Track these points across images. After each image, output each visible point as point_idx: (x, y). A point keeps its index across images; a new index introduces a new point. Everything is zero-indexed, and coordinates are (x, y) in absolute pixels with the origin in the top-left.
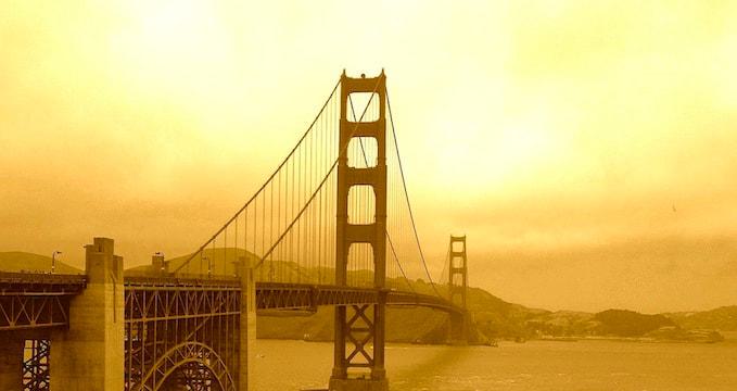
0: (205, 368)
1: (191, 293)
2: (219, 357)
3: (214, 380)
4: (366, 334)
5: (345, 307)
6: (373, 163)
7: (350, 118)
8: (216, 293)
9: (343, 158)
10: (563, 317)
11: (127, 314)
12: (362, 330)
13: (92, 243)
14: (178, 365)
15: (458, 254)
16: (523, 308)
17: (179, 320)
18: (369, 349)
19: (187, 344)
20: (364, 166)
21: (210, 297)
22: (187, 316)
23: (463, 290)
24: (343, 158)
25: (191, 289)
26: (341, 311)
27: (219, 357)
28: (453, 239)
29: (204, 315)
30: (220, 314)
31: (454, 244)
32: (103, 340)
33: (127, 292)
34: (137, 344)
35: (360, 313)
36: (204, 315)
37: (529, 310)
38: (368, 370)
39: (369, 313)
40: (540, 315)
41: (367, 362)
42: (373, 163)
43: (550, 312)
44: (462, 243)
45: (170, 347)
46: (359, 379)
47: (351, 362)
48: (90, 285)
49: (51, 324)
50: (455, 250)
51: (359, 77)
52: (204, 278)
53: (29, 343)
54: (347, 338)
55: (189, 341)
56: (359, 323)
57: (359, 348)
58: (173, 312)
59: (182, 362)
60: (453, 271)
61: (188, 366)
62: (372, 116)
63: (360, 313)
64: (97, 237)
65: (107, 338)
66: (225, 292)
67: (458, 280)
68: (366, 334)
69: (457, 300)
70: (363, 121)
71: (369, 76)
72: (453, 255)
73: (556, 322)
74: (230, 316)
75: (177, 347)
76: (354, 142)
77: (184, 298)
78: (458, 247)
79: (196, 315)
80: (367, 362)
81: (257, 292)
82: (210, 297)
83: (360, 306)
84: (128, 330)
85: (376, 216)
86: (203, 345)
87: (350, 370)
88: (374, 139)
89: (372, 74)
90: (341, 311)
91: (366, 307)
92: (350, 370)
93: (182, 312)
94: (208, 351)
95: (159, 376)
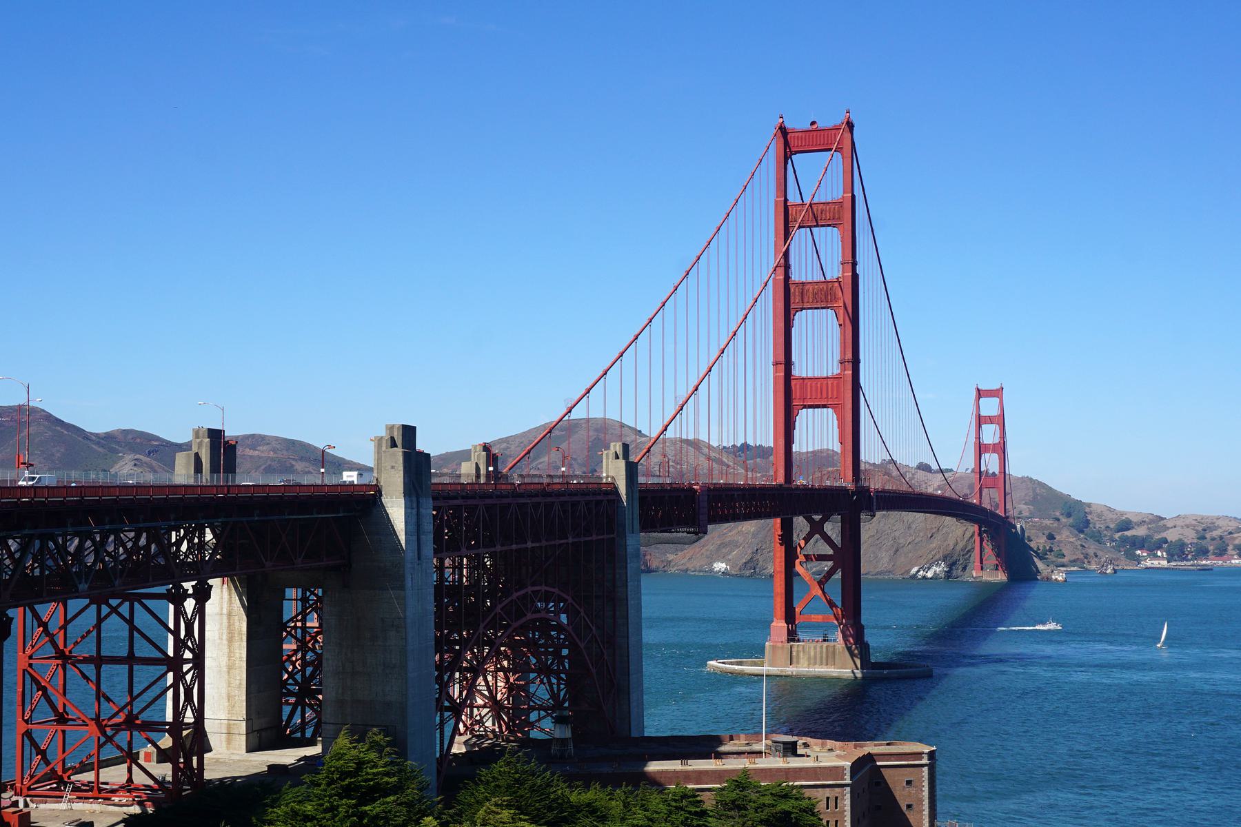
0: (560, 628)
2: (582, 610)
3: (573, 647)
5: (792, 519)
6: (834, 271)
7: (793, 198)
8: (574, 505)
10: (1188, 526)
12: (821, 558)
15: (990, 420)
16: (1111, 510)
19: (530, 589)
20: (818, 277)
22: (529, 545)
23: (1002, 480)
25: (535, 500)
26: (787, 528)
27: (582, 610)
28: (980, 394)
29: (558, 542)
30: (582, 539)
32: (402, 588)
34: (455, 590)
36: (558, 542)
37: (1122, 515)
39: (833, 528)
42: (834, 271)
43: (1162, 519)
44: (996, 400)
50: (982, 414)
51: (807, 126)
53: (291, 593)
59: (523, 620)
60: (981, 449)
62: (833, 191)
63: (817, 529)
65: (409, 583)
66: (587, 503)
67: (991, 463)
68: (827, 565)
69: (989, 499)
70: (816, 200)
71: (821, 124)
72: (980, 421)
73: (1172, 536)
75: (515, 595)
78: (989, 407)
79: (544, 543)
85: (842, 362)
89: (830, 119)
90: (787, 528)
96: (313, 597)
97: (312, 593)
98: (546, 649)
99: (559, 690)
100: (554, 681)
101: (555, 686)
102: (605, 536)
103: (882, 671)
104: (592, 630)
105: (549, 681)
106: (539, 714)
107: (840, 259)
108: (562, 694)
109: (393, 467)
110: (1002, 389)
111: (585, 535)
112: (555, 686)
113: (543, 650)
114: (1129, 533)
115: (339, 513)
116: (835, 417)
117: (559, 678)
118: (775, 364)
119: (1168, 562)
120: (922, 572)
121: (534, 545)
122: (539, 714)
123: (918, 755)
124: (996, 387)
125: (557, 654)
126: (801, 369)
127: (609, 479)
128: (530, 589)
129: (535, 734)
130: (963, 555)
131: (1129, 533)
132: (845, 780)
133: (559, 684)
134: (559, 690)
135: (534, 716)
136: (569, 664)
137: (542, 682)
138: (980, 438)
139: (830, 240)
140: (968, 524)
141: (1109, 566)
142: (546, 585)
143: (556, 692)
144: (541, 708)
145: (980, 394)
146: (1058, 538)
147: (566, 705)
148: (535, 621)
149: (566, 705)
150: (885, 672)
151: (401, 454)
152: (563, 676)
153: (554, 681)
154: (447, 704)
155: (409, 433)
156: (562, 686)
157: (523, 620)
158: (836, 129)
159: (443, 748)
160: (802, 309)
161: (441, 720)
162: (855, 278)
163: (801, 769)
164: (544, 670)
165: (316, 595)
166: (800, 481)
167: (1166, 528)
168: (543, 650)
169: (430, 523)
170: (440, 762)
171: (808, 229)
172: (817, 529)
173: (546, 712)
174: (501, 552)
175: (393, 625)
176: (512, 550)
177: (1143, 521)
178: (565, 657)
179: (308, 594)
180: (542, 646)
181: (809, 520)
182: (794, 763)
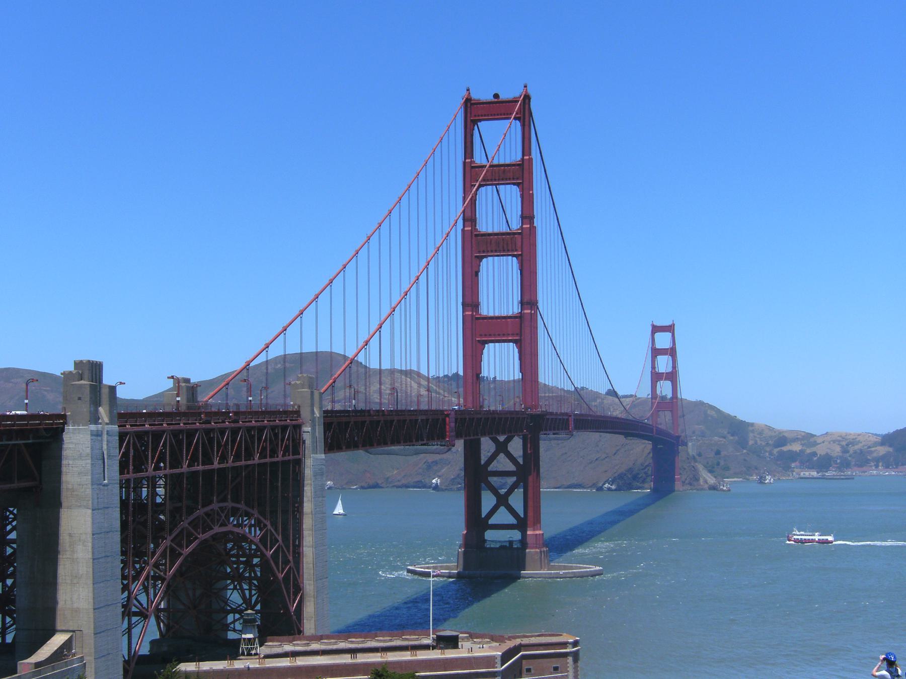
1: (222, 432)
4: (511, 480)
5: (479, 440)
6: (515, 225)
9: (470, 217)
10: (834, 442)
11: (123, 467)
13: (71, 368)
14: (202, 537)
15: (663, 352)
16: (770, 429)
17: (204, 472)
18: (516, 500)
20: (504, 229)
21: (252, 437)
22: (216, 465)
23: (672, 404)
24: (470, 217)
27: (268, 523)
28: (656, 329)
30: (268, 460)
31: (658, 335)
33: (122, 436)
34: (140, 507)
35: (502, 448)
37: (780, 432)
38: (516, 535)
39: (516, 446)
40: (795, 440)
41: (512, 520)
42: (515, 225)
43: (813, 436)
44: (669, 335)
45: (190, 511)
46: (502, 547)
47: (492, 521)
48: (69, 428)
49: (16, 485)
50: (658, 346)
51: (490, 98)
52: (243, 409)
54: (483, 485)
55: (219, 502)
56: (502, 463)
57: (502, 501)
58: (193, 461)
59: (211, 533)
60: (656, 377)
61: (223, 537)
62: (512, 155)
64: (79, 358)
67: (665, 388)
69: (665, 420)
70: (495, 162)
71: (503, 96)
72: (656, 352)
73: (821, 450)
74: (284, 462)
76: (486, 195)
77: (211, 440)
78: (663, 341)
80: (512, 520)
81: (327, 426)
82: (252, 437)
83: (502, 438)
84: (124, 485)
85: (522, 303)
86: (242, 506)
87: (490, 535)
88: (515, 188)
91: (509, 440)
92: (490, 535)
93: (208, 460)
94: (253, 515)
95: (174, 555)
96: (11, 516)
97: (12, 513)
98: (238, 560)
99: (251, 596)
100: (245, 587)
101: (247, 592)
102: (291, 457)
103: (558, 571)
104: (278, 541)
105: (241, 587)
106: (234, 616)
107: (520, 213)
108: (254, 599)
109: (80, 399)
110: (674, 325)
111: (271, 457)
112: (247, 592)
113: (234, 559)
114: (785, 449)
115: (29, 440)
116: (516, 350)
117: (250, 584)
118: (464, 304)
119: (818, 473)
120: (607, 485)
121: (222, 466)
122: (234, 616)
123: (564, 645)
124: (667, 323)
125: (248, 564)
126: (487, 309)
127: (296, 407)
128: (215, 506)
129: (231, 635)
130: (642, 469)
131: (785, 449)
132: (496, 668)
133: (250, 590)
134: (251, 596)
135: (230, 618)
136: (261, 572)
137: (235, 588)
138: (655, 368)
139: (511, 194)
140: (647, 442)
141: (767, 477)
142: (233, 501)
143: (248, 597)
144: (234, 611)
145: (656, 329)
146: (723, 453)
147: (258, 607)
148: (226, 534)
149: (258, 607)
150: (561, 572)
151: (88, 386)
152: (255, 582)
153: (245, 587)
154: (134, 609)
155: (94, 369)
156: (254, 592)
157: (211, 533)
158: (515, 101)
159: (131, 652)
160: (486, 257)
161: (129, 624)
162: (532, 230)
163: (456, 659)
164: (238, 578)
165: (13, 514)
166: (398, 409)
167: (815, 444)
168: (234, 559)
169: (116, 448)
170: (127, 663)
171: (494, 187)
172: (502, 448)
173: (240, 614)
174: (188, 473)
175: (80, 540)
176: (197, 472)
177: (797, 438)
178: (256, 565)
179: (8, 513)
180: (233, 556)
181: (495, 440)
182: (451, 654)
